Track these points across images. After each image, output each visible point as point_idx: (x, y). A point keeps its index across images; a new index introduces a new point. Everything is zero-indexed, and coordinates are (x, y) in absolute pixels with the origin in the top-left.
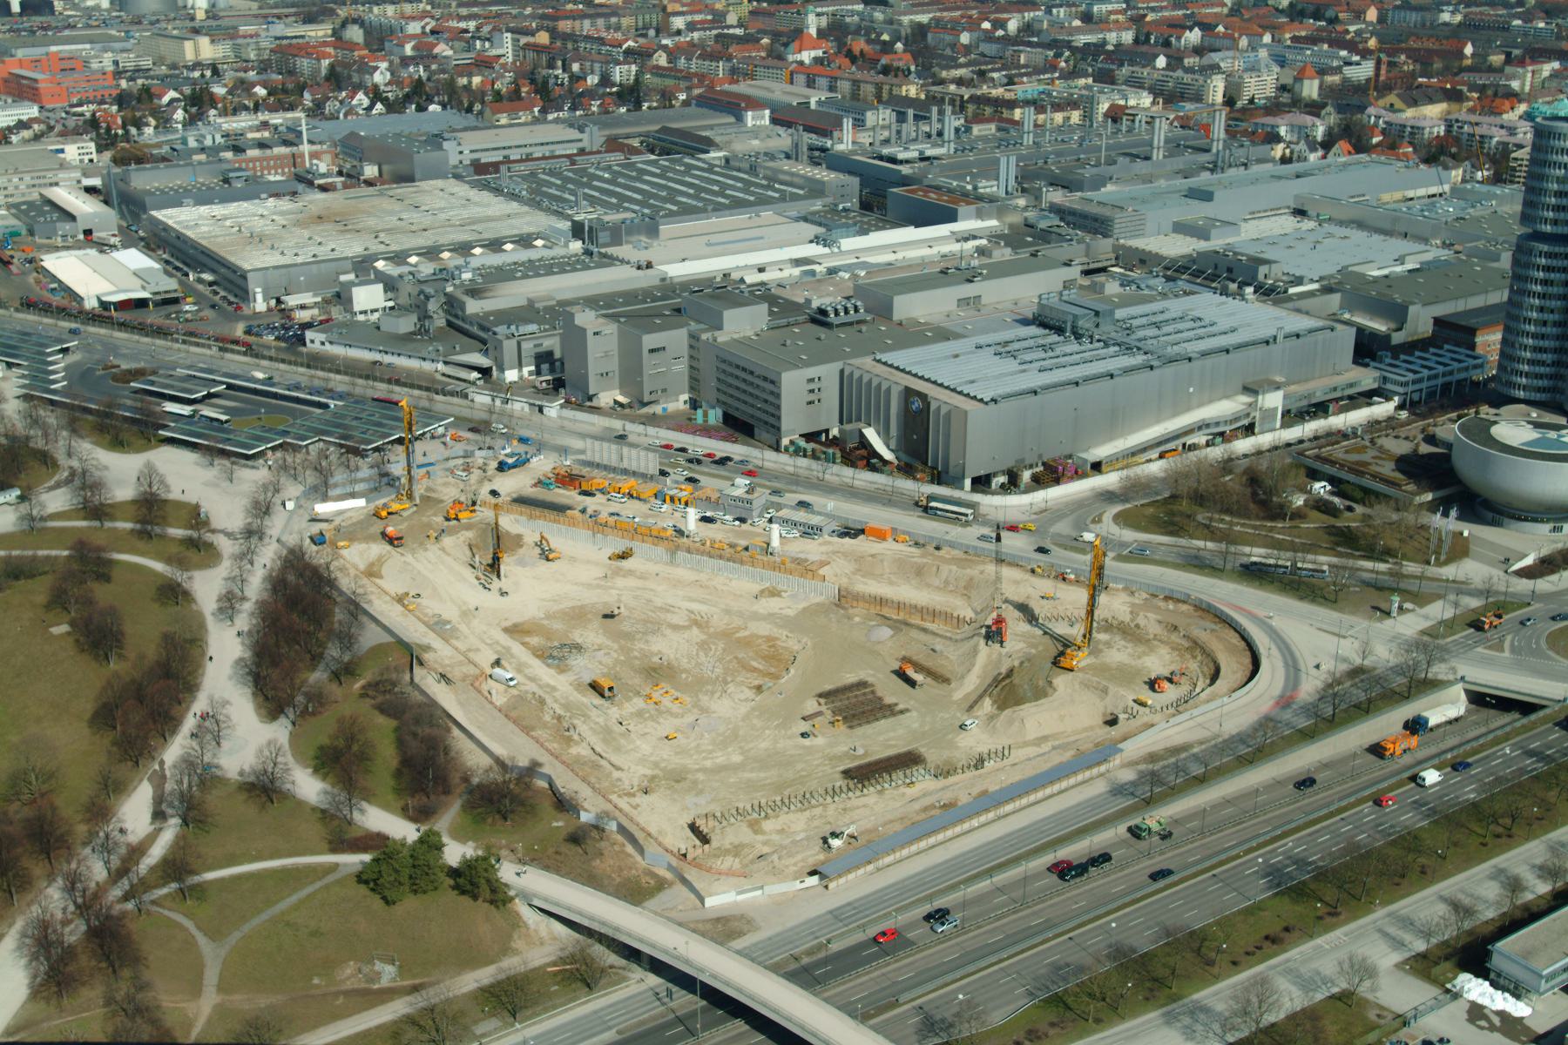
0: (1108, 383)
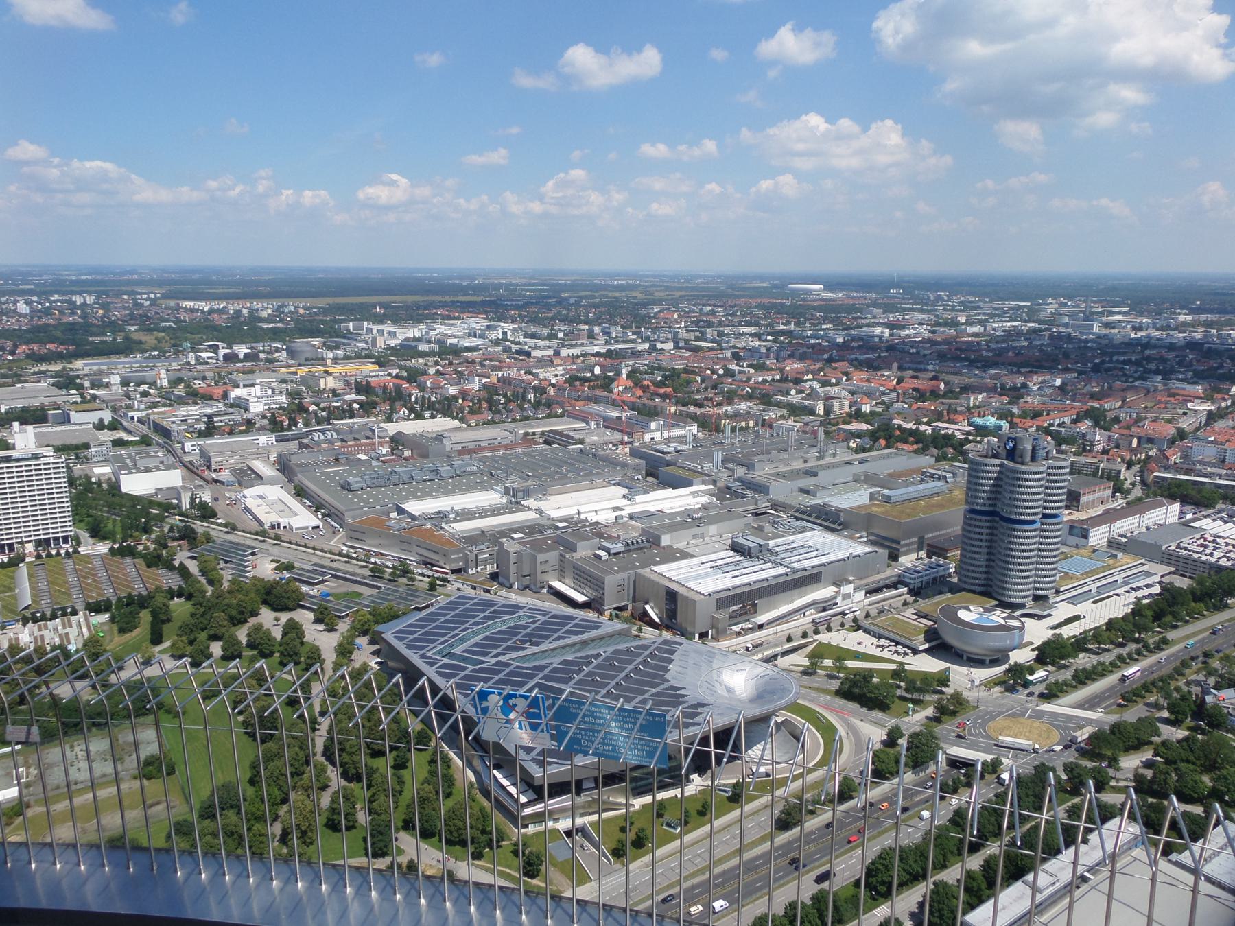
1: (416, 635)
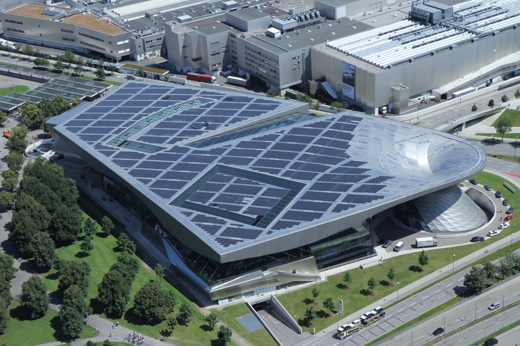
0: (449, 51)
1: (89, 126)
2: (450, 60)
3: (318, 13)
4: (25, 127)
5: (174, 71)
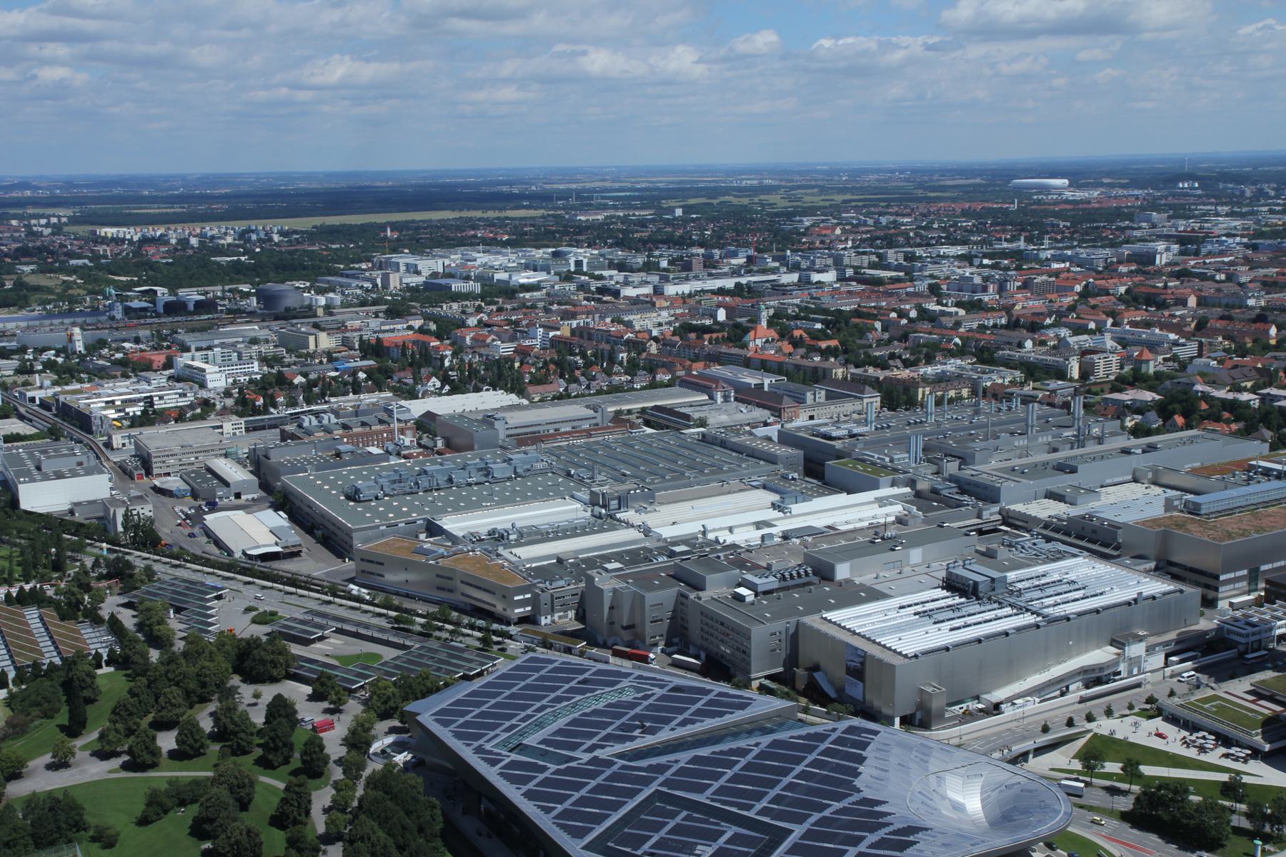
1: (468, 718)
2: (1003, 655)
3: (809, 569)
4: (373, 715)
5: (593, 643)
